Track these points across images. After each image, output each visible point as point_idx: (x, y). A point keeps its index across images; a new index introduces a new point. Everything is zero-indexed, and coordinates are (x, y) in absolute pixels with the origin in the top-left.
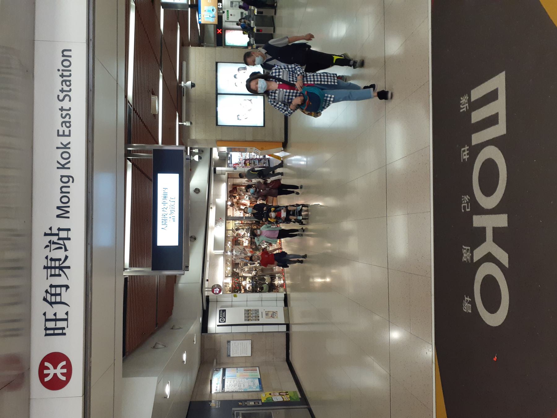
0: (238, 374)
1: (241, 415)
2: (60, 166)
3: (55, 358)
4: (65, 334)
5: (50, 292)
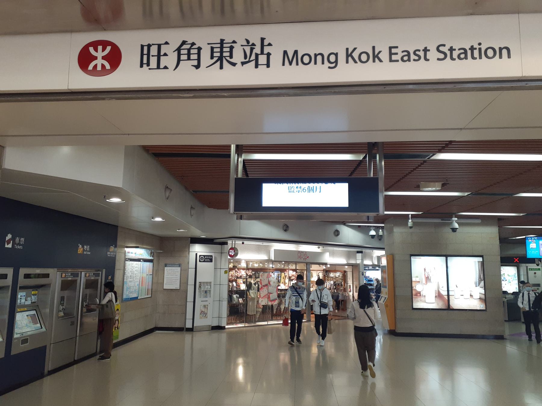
0: (145, 275)
1: (97, 278)
2: (350, 52)
3: (115, 58)
4: (141, 66)
5: (193, 47)
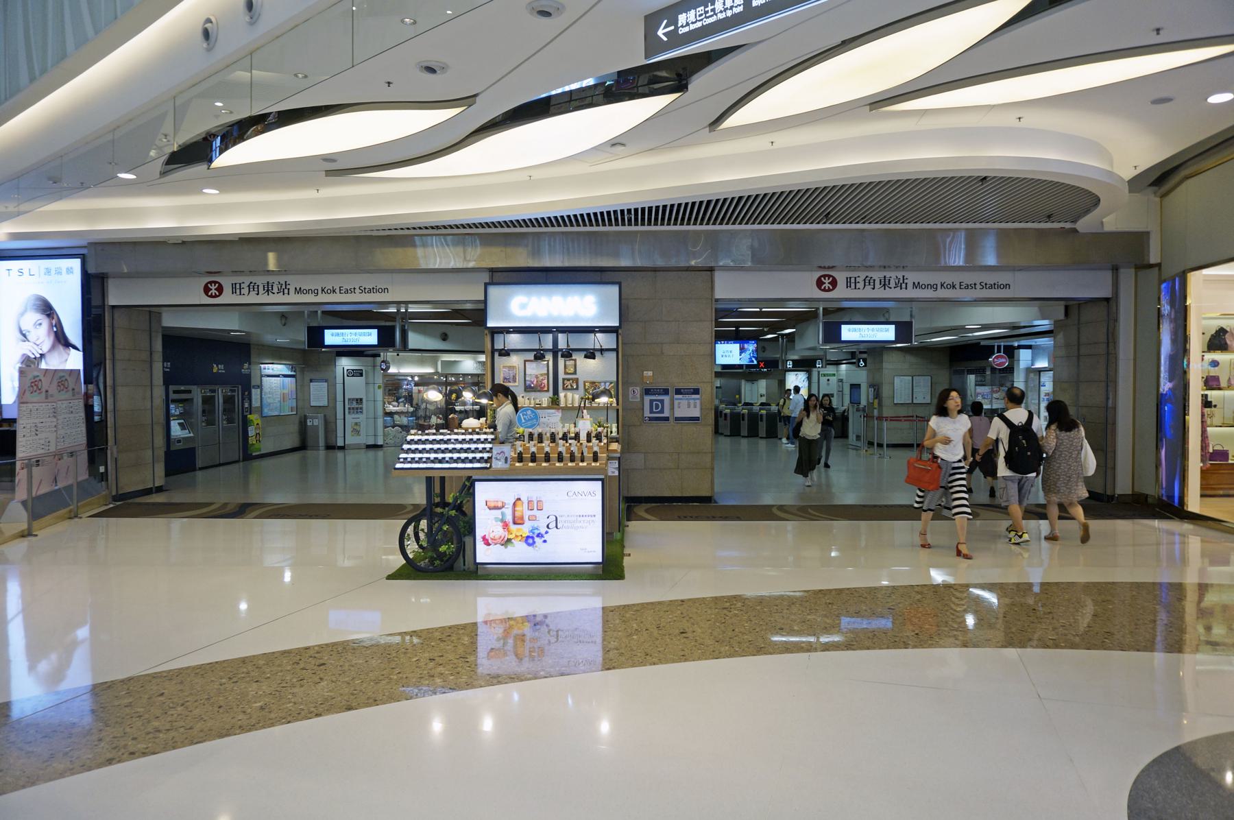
3: (834, 283)
